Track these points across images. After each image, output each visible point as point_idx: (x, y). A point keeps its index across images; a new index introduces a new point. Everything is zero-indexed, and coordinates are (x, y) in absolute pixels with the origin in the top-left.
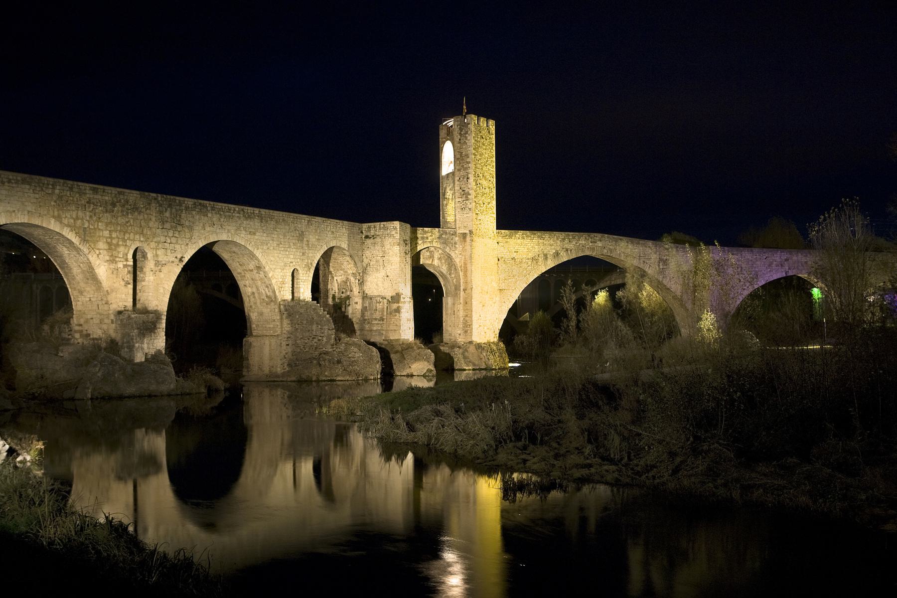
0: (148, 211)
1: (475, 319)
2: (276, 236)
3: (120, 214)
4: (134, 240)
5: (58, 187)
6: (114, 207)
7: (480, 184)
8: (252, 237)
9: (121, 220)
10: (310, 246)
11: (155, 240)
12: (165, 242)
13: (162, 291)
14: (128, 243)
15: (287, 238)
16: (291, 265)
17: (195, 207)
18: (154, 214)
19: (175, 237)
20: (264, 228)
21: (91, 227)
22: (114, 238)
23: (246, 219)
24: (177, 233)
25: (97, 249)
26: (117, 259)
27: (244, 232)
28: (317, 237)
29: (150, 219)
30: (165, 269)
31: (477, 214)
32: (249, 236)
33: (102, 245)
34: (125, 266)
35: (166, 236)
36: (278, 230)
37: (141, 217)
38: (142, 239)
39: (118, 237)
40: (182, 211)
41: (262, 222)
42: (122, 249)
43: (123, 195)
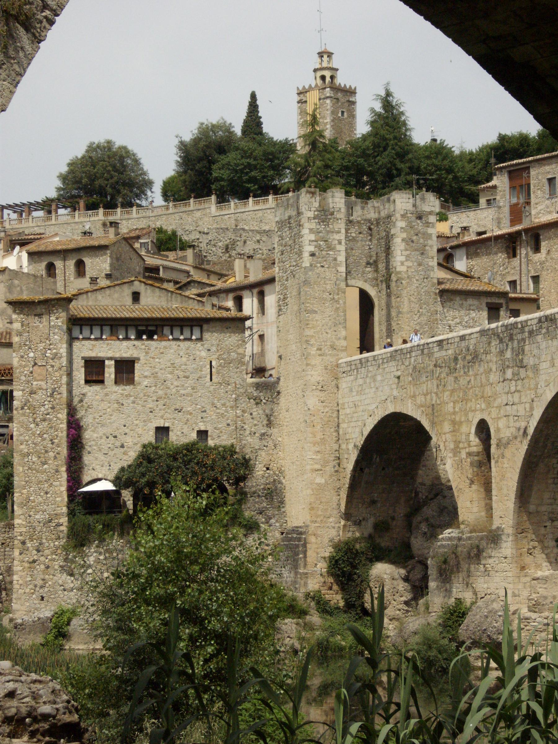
0: (488, 357)
3: (462, 372)
4: (475, 411)
5: (413, 354)
6: (456, 364)
12: (507, 404)
13: (505, 491)
14: (470, 415)
17: (541, 327)
18: (494, 359)
19: (518, 391)
21: (438, 402)
22: (457, 412)
24: (519, 382)
25: (445, 434)
26: (461, 445)
29: (491, 370)
30: (508, 453)
33: (447, 427)
34: (469, 454)
35: (508, 393)
37: (482, 370)
38: (483, 406)
39: (461, 410)
40: (525, 343)
42: (464, 429)
43: (464, 340)
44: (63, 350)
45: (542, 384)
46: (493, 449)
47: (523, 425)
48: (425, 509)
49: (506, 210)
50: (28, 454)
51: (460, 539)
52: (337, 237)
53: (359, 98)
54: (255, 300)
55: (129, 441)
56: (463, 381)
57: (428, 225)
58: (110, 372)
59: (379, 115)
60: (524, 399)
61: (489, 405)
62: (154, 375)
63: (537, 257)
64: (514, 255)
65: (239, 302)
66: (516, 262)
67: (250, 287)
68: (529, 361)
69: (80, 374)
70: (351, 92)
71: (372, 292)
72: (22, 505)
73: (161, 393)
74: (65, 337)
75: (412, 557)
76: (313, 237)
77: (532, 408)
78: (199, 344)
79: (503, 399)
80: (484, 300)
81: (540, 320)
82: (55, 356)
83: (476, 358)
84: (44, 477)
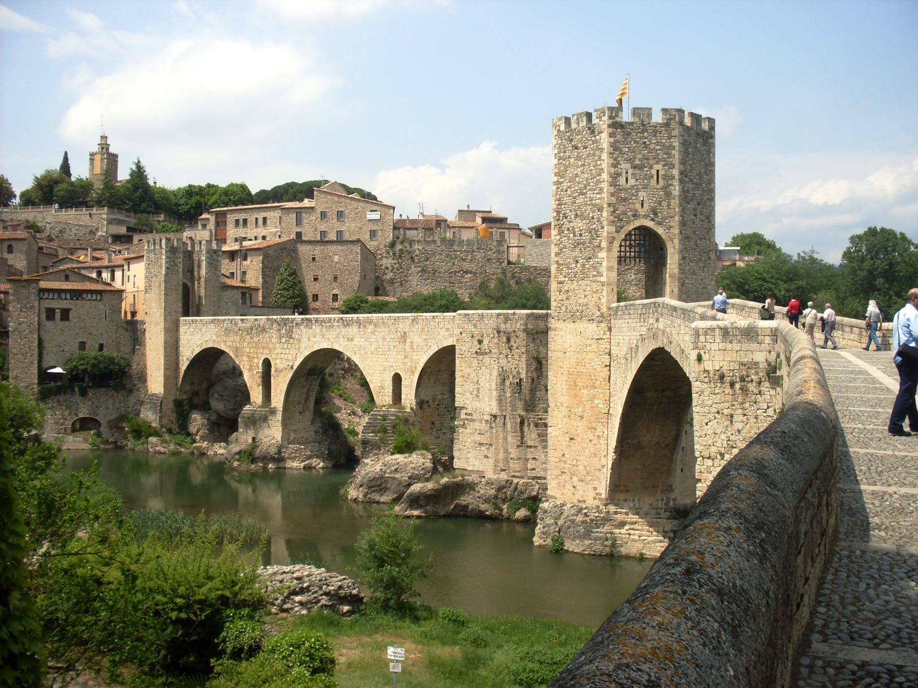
1: (554, 459)
2: (374, 340)
7: (568, 230)
8: (350, 343)
9: (256, 339)
10: (415, 347)
11: (276, 351)
13: (279, 392)
15: (388, 340)
16: (392, 369)
20: (362, 333)
23: (345, 326)
27: (342, 339)
28: (424, 337)
30: (281, 375)
31: (561, 283)
32: (347, 343)
33: (245, 358)
34: (258, 372)
36: (376, 333)
37: (267, 336)
41: (360, 327)
42: (255, 360)
44: (36, 304)
45: (302, 347)
46: (273, 372)
47: (291, 364)
48: (216, 386)
49: (214, 231)
50: (17, 354)
51: (256, 411)
52: (179, 260)
53: (119, 159)
54: (109, 274)
55: (66, 349)
56: (256, 339)
57: (218, 256)
58: (58, 315)
59: (134, 171)
60: (291, 352)
61: (270, 352)
62: (79, 317)
63: (245, 263)
64: (233, 260)
65: (99, 274)
66: (234, 264)
67: (107, 267)
68: (295, 336)
69: (44, 316)
70: (116, 156)
71: (190, 285)
72: (13, 378)
73: (82, 325)
74: (38, 298)
75: (210, 409)
76: (168, 260)
77: (296, 357)
78: (100, 303)
79: (280, 351)
80: (241, 290)
81: (303, 319)
82: (32, 307)
83: (264, 330)
84: (25, 365)
